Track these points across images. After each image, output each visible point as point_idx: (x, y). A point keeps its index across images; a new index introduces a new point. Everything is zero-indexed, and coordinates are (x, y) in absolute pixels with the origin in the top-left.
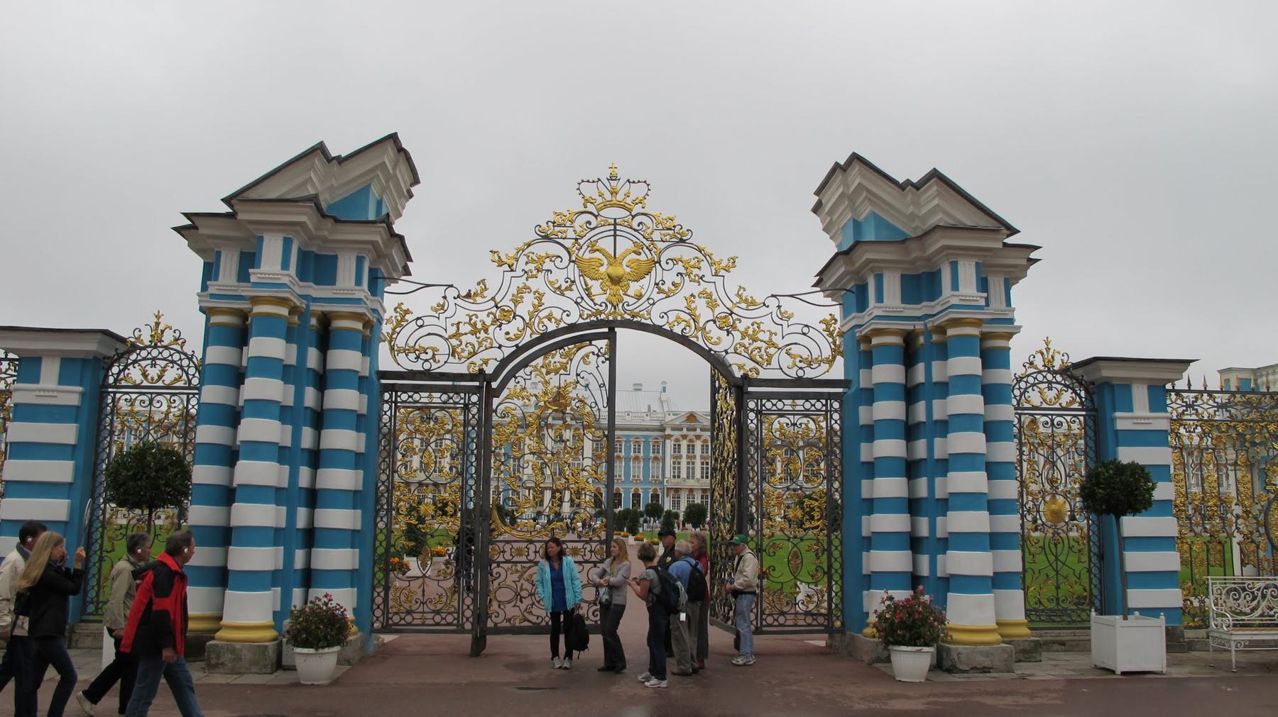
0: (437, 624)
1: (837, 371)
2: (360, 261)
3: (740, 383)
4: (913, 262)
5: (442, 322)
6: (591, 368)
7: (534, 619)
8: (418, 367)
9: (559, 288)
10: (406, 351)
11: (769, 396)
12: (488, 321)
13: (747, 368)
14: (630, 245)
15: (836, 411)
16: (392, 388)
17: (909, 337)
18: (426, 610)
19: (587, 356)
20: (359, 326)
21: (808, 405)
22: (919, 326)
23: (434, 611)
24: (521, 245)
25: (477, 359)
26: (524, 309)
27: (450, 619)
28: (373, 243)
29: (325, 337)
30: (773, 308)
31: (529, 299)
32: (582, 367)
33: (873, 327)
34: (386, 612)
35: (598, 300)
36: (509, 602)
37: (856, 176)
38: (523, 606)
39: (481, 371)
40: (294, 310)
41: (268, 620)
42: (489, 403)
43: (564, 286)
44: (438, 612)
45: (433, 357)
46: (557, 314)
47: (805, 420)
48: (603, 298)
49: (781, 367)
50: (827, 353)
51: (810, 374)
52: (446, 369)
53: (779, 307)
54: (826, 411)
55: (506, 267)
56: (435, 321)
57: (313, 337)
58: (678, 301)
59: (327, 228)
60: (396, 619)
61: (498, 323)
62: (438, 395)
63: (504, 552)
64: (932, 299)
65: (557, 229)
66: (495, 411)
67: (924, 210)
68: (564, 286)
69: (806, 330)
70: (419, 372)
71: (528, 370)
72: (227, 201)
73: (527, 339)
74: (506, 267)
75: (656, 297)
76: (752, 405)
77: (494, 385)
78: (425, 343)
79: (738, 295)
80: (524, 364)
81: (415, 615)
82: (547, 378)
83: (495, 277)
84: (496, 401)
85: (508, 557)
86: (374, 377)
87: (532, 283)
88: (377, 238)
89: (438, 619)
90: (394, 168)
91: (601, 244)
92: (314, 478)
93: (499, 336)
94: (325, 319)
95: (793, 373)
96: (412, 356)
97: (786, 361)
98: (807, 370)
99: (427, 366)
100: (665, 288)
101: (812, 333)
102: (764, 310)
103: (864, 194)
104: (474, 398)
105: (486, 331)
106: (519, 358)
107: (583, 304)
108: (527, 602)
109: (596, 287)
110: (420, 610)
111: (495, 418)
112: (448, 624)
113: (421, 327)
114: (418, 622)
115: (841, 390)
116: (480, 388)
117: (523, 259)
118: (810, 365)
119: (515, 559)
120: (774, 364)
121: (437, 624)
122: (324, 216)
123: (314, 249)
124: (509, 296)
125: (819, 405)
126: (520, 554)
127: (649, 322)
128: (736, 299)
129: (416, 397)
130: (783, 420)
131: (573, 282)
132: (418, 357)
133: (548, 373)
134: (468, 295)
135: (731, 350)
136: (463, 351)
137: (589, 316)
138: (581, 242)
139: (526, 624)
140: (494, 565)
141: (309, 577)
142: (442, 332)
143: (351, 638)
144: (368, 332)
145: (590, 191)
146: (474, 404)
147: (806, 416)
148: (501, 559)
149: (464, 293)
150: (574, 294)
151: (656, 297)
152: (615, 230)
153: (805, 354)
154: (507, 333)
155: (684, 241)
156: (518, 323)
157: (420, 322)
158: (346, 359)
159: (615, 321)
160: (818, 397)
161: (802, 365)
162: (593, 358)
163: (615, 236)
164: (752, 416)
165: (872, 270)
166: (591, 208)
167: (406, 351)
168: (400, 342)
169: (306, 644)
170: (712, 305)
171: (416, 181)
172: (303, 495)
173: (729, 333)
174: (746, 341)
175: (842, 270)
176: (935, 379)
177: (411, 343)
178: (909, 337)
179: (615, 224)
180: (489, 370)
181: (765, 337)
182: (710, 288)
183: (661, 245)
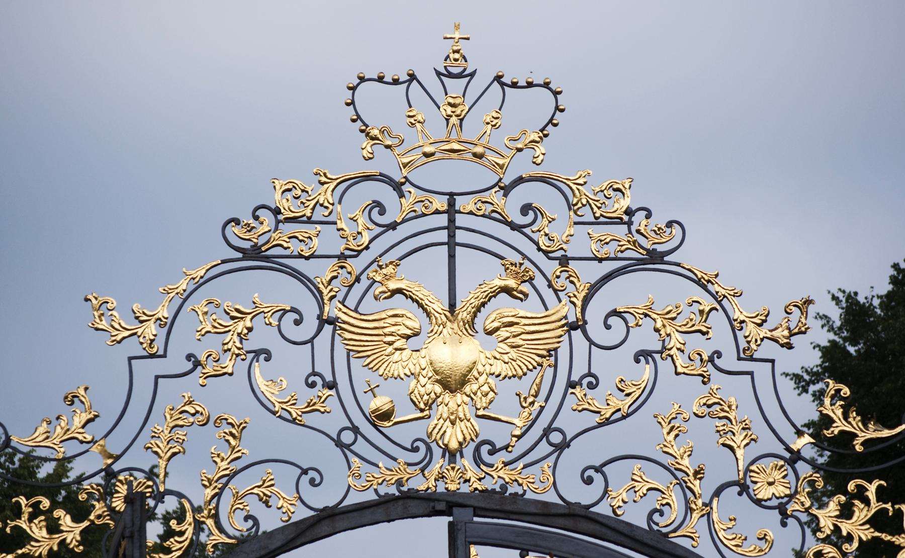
107: (361, 446)
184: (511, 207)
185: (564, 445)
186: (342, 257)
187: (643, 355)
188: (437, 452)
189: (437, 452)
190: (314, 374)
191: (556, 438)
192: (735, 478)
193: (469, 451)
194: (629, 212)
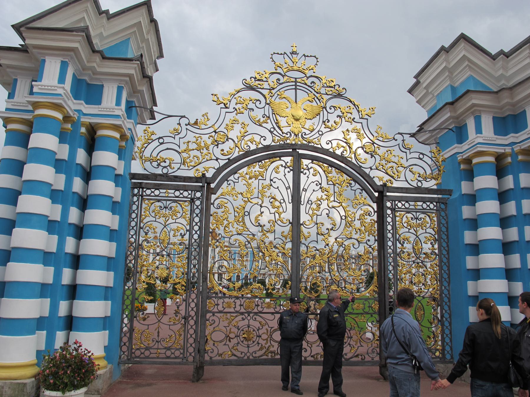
0: (168, 357)
2: (120, 90)
3: (381, 189)
4: (501, 108)
5: (177, 141)
6: (281, 176)
7: (238, 354)
8: (159, 171)
9: (259, 121)
10: (151, 160)
11: (400, 199)
12: (209, 142)
13: (385, 180)
16: (140, 186)
17: (499, 158)
18: (160, 346)
20: (117, 135)
21: (425, 206)
22: (508, 150)
23: (165, 348)
25: (201, 168)
27: (177, 353)
28: (130, 76)
29: (92, 143)
30: (400, 141)
31: (237, 128)
32: (274, 175)
33: (479, 149)
34: (130, 348)
35: (285, 130)
36: (221, 341)
37: (462, 51)
38: (231, 345)
39: (204, 175)
40: (67, 118)
41: (32, 358)
42: (208, 199)
43: (262, 120)
44: (168, 349)
45: (170, 165)
46: (257, 138)
47: (422, 216)
51: (426, 185)
52: (179, 173)
53: (403, 140)
55: (222, 105)
56: (171, 140)
57: (83, 142)
58: (338, 134)
59: (96, 63)
60: (138, 353)
61: (216, 143)
62: (173, 191)
63: (218, 305)
64: (517, 131)
65: (258, 82)
66: (213, 204)
67: (510, 72)
68: (262, 120)
69: (421, 156)
70: (160, 175)
71: (236, 176)
72: (17, 28)
73: (236, 154)
75: (324, 130)
76: (389, 204)
77: (213, 186)
78: (163, 155)
80: (234, 172)
81: (152, 351)
82: (250, 181)
83: (214, 111)
84: (213, 197)
85: (220, 308)
86: (128, 177)
87: (241, 118)
88: (132, 72)
89: (169, 353)
90: (148, 33)
92: (78, 246)
93: (217, 152)
94: (92, 130)
95: (414, 184)
96: (155, 164)
98: (423, 182)
99: (165, 171)
100: (329, 124)
101: (426, 159)
102: (393, 143)
103: (467, 63)
104: (198, 194)
106: (231, 167)
107: (275, 132)
108: (235, 341)
109: (283, 122)
110: (156, 346)
111: (213, 210)
112: (176, 358)
113: (161, 144)
114: (154, 355)
116: (203, 186)
117: (234, 101)
118: (425, 179)
119: (226, 310)
121: (168, 357)
122: (94, 51)
123: (86, 78)
124: (224, 125)
125: (432, 206)
126: (229, 307)
127: (319, 146)
129: (157, 192)
130: (410, 215)
131: (269, 117)
132: (159, 165)
133: (250, 178)
134: (196, 123)
135: (374, 167)
137: (278, 141)
139: (234, 358)
140: (208, 315)
141: (70, 323)
142: (177, 148)
143: (99, 372)
144: (124, 144)
147: (423, 213)
148: (216, 310)
149: (192, 122)
150: (269, 126)
151: (324, 130)
153: (422, 172)
154: (222, 150)
155: (341, 95)
156: (230, 143)
157: (161, 141)
158: (106, 158)
159: (296, 144)
161: (420, 179)
162: (281, 169)
163: (296, 89)
164: (389, 212)
165: (472, 113)
166: (280, 70)
167: (151, 160)
168: (147, 154)
169: (54, 388)
170: (359, 137)
171: (161, 56)
172: (69, 259)
173: (372, 156)
174: (383, 162)
175: (448, 115)
176: (522, 185)
177: (154, 154)
178: (499, 158)
179: (296, 82)
180: (209, 175)
183: (326, 97)
184: (308, 82)
185: (322, 134)
186: (270, 89)
187: (338, 116)
188: (293, 135)
189: (293, 135)
190: (264, 114)
192: (361, 146)
193: (300, 135)
194: (334, 86)
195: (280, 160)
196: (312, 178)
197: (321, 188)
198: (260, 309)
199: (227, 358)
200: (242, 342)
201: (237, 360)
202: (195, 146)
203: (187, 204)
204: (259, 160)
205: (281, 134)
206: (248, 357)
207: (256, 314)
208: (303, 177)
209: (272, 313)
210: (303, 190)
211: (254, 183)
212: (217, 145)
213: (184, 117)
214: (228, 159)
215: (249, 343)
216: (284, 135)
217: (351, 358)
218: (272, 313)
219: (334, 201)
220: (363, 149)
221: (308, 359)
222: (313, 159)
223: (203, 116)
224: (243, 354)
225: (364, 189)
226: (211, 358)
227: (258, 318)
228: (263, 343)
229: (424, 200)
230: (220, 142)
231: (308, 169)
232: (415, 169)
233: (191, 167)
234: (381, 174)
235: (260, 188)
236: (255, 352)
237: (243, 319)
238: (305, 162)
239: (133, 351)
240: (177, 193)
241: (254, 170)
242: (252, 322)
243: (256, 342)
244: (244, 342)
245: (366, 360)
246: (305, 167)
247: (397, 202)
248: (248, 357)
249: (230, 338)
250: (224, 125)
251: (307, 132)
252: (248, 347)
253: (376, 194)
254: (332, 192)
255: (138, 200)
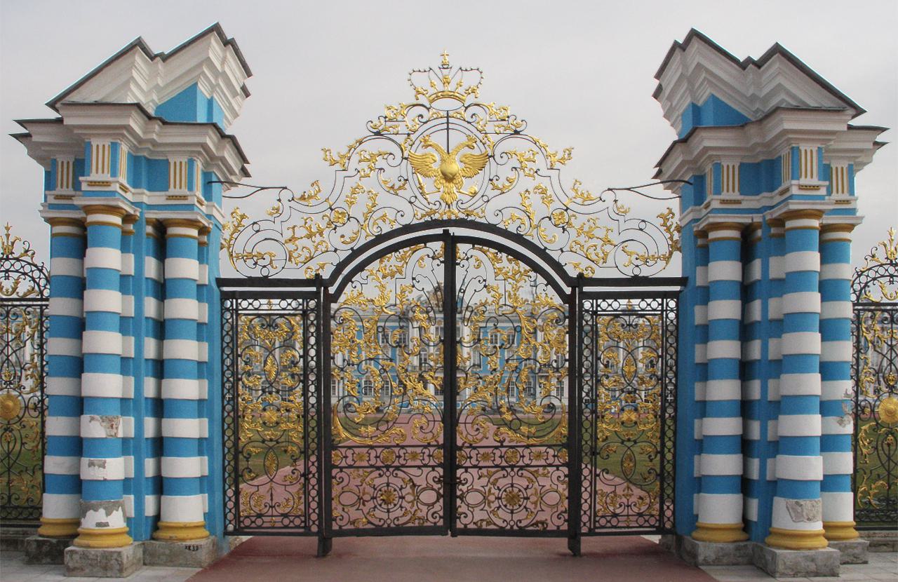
0: (286, 527)
1: (675, 269)
5: (277, 226)
6: (427, 271)
7: (377, 522)
8: (256, 273)
11: (605, 296)
12: (323, 225)
13: (583, 267)
14: (464, 139)
15: (672, 310)
19: (422, 259)
24: (352, 142)
25: (314, 265)
26: (357, 211)
27: (297, 522)
30: (609, 203)
32: (418, 270)
34: (237, 516)
36: (352, 505)
39: (317, 275)
42: (327, 309)
43: (398, 184)
44: (285, 516)
46: (391, 215)
48: (437, 197)
49: (619, 266)
50: (664, 249)
51: (646, 272)
54: (662, 311)
58: (512, 198)
62: (277, 301)
65: (389, 124)
74: (338, 167)
75: (490, 193)
76: (587, 305)
77: (332, 290)
79: (576, 191)
82: (383, 282)
83: (327, 176)
84: (334, 306)
91: (432, 140)
95: (629, 272)
97: (622, 259)
98: (643, 267)
102: (600, 205)
104: (312, 303)
105: (321, 234)
107: (417, 203)
108: (371, 504)
109: (428, 185)
110: (270, 513)
115: (677, 288)
117: (355, 158)
120: (610, 262)
124: (343, 197)
125: (654, 305)
128: (572, 194)
132: (256, 263)
134: (303, 198)
136: (299, 256)
137: (423, 216)
138: (413, 137)
142: (278, 237)
145: (421, 81)
146: (312, 310)
149: (298, 195)
152: (448, 123)
153: (642, 251)
154: (343, 236)
156: (353, 226)
160: (653, 296)
161: (638, 262)
166: (423, 100)
180: (326, 275)
181: (600, 233)
182: (545, 183)
185: (488, 201)
186: (409, 135)
188: (443, 204)
191: (485, 199)
195: (426, 247)
196: (473, 272)
197: (485, 286)
198: (402, 462)
199: (361, 527)
200: (380, 505)
201: (372, 529)
202: (304, 232)
203: (298, 318)
204: (395, 248)
205: (427, 205)
206: (389, 525)
207: (397, 468)
208: (460, 272)
209: (419, 467)
210: (460, 290)
211: (390, 284)
212: (335, 229)
213: (285, 188)
214: (352, 249)
215: (390, 507)
216: (431, 206)
217: (526, 526)
218: (419, 467)
219: (505, 305)
220: (550, 219)
221: (468, 526)
222: (473, 241)
223: (313, 185)
224: (382, 522)
225: (551, 282)
226: (340, 527)
227: (400, 474)
228: (408, 506)
229: (643, 296)
230: (338, 224)
231: (467, 259)
232: (631, 246)
233: (300, 265)
234: (574, 258)
235: (399, 292)
236: (397, 518)
237: (380, 476)
238: (462, 248)
239: (242, 519)
240: (284, 304)
241: (388, 264)
242: (392, 480)
243: (398, 506)
244: (383, 506)
245: (548, 529)
246: (462, 256)
247: (599, 301)
248: (389, 525)
249: (364, 501)
250: (343, 197)
251: (465, 199)
252: (388, 511)
253: (568, 290)
254: (501, 291)
255: (232, 316)
